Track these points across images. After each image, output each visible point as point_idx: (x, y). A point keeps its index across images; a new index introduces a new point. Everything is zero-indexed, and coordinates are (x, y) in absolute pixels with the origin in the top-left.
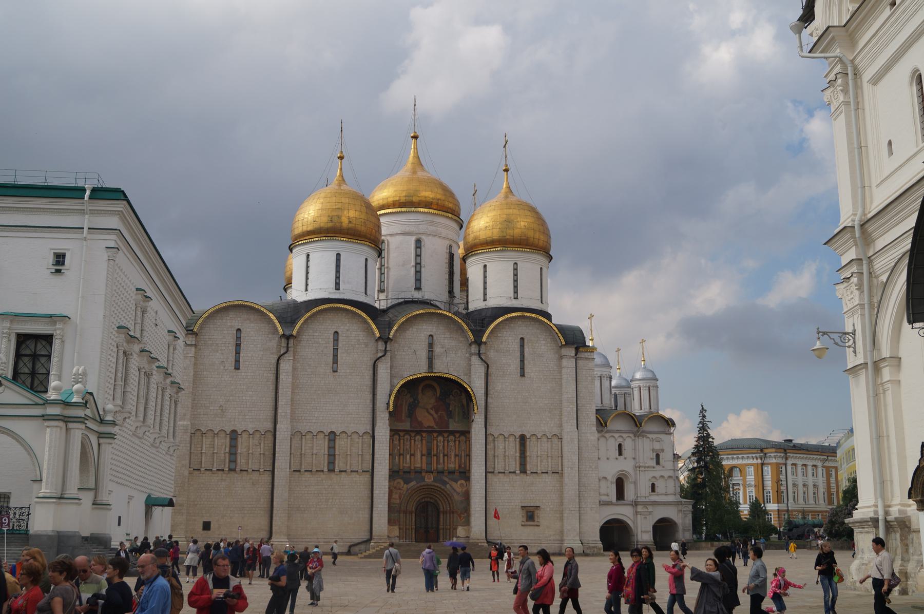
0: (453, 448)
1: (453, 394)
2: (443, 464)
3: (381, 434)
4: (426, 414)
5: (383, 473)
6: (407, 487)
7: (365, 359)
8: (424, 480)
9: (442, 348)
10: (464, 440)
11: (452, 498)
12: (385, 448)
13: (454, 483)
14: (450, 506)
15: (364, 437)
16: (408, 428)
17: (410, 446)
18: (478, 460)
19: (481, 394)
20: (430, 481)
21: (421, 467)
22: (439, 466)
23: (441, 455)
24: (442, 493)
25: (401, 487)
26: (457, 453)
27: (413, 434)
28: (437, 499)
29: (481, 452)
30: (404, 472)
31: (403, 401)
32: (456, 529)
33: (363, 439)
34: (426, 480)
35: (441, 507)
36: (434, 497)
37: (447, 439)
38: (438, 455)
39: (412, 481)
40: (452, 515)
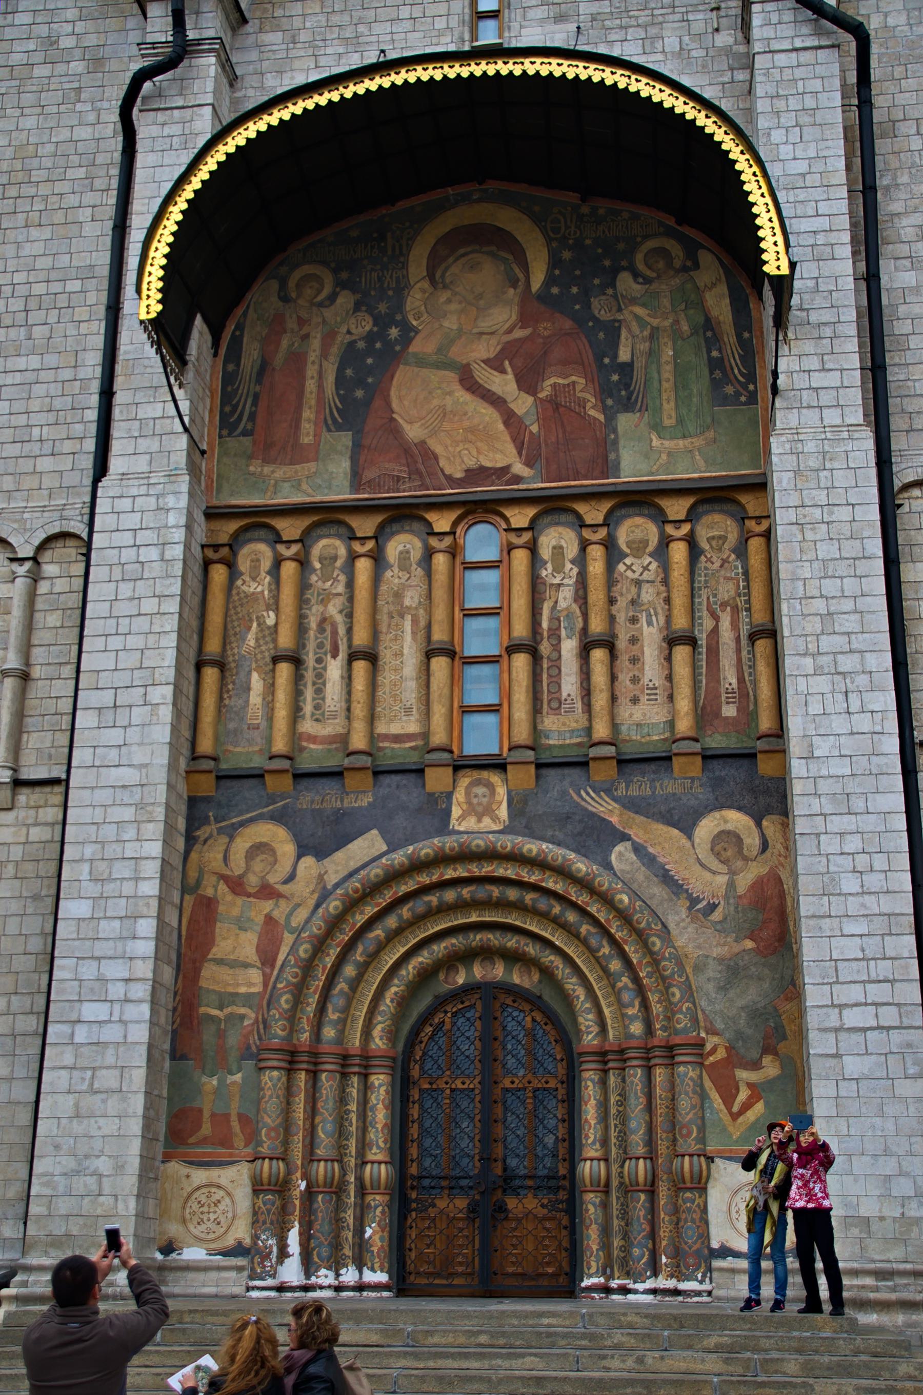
0: (648, 594)
1: (641, 266)
2: (579, 705)
3: (133, 520)
4: (463, 396)
5: (130, 776)
6: (321, 877)
7: (83, 133)
8: (443, 828)
9: (560, 18)
10: (733, 537)
11: (657, 943)
12: (149, 606)
13: (661, 829)
14: (645, 1005)
15: (50, 569)
16: (341, 494)
17: (351, 599)
18: (826, 643)
19: (822, 223)
20: (487, 823)
21: (425, 735)
22: (549, 722)
23: (569, 647)
24: (582, 911)
25: (274, 879)
26: (681, 622)
27: (365, 525)
28: (550, 959)
29: (850, 585)
30: (298, 776)
31: (306, 337)
32: (700, 1185)
33: (35, 577)
34: (454, 823)
35: (587, 1020)
36: (532, 949)
37: (602, 533)
38: (545, 648)
39: (360, 833)
40: (660, 1075)
